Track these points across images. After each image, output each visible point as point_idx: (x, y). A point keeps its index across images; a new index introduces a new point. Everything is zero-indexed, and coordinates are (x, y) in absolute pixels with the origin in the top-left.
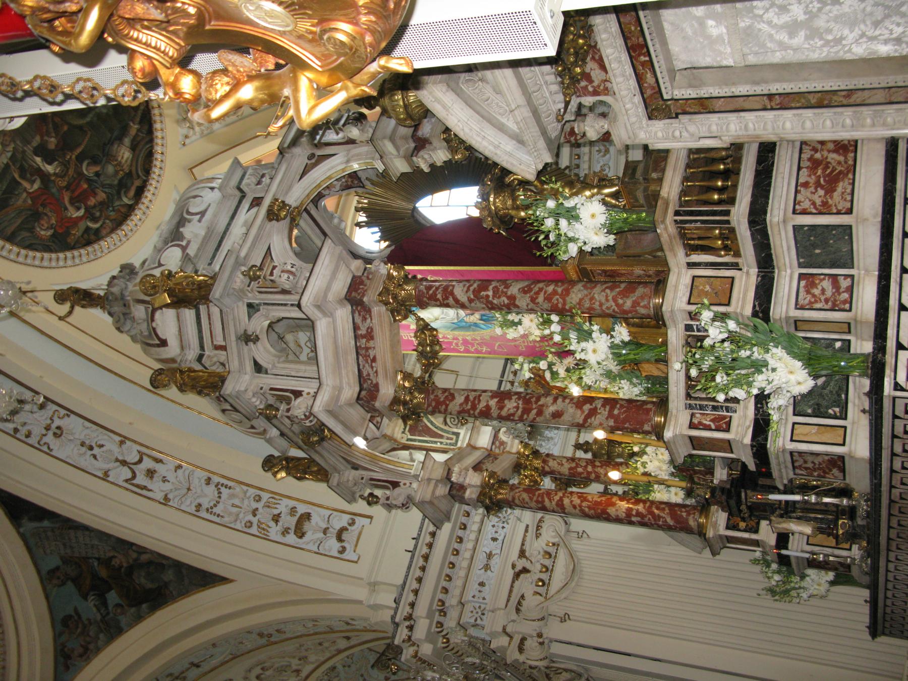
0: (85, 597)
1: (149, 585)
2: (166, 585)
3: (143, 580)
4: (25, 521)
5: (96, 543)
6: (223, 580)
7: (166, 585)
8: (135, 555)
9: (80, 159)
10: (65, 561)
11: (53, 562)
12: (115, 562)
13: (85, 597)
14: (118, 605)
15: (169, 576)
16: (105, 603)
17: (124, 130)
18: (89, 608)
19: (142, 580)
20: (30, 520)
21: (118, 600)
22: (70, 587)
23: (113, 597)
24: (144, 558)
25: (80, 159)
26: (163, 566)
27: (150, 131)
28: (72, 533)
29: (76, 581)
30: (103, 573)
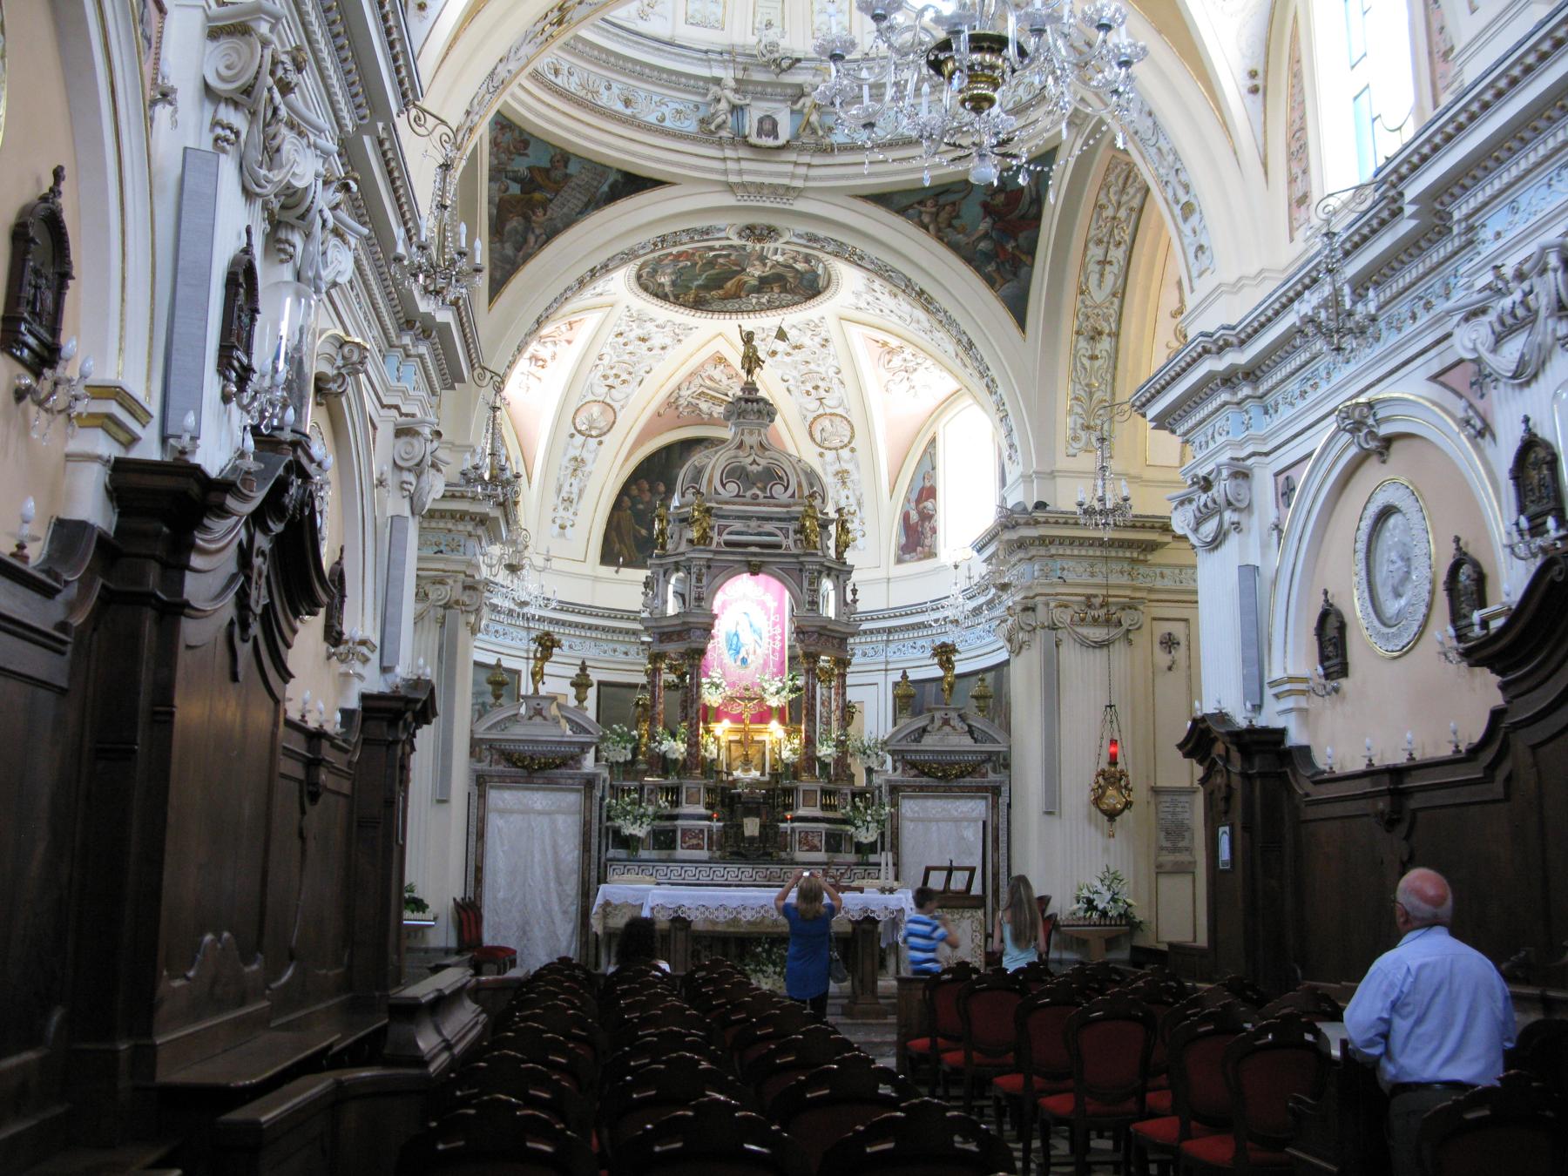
0: (529, 169)
1: (508, 227)
2: (502, 242)
3: (514, 223)
4: (619, 177)
5: (565, 210)
6: (491, 300)
7: (502, 242)
8: (538, 231)
9: (694, 265)
10: (567, 177)
11: (572, 169)
12: (540, 212)
13: (529, 169)
14: (507, 189)
15: (509, 250)
16: (515, 180)
17: (674, 283)
18: (520, 165)
19: (514, 223)
20: (616, 181)
21: (511, 191)
22: (545, 163)
23: (515, 189)
24: (532, 239)
25: (694, 265)
26: (518, 249)
27: (656, 295)
28: (585, 200)
29: (547, 171)
30: (537, 196)
